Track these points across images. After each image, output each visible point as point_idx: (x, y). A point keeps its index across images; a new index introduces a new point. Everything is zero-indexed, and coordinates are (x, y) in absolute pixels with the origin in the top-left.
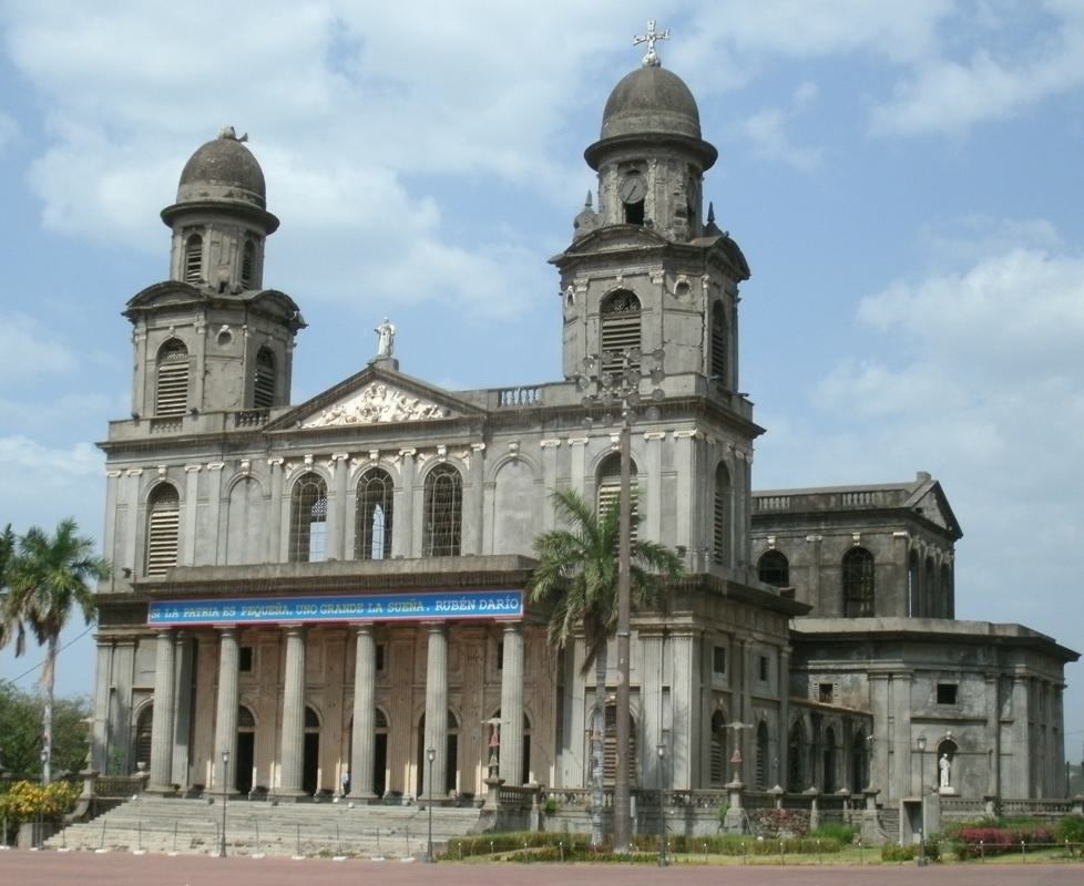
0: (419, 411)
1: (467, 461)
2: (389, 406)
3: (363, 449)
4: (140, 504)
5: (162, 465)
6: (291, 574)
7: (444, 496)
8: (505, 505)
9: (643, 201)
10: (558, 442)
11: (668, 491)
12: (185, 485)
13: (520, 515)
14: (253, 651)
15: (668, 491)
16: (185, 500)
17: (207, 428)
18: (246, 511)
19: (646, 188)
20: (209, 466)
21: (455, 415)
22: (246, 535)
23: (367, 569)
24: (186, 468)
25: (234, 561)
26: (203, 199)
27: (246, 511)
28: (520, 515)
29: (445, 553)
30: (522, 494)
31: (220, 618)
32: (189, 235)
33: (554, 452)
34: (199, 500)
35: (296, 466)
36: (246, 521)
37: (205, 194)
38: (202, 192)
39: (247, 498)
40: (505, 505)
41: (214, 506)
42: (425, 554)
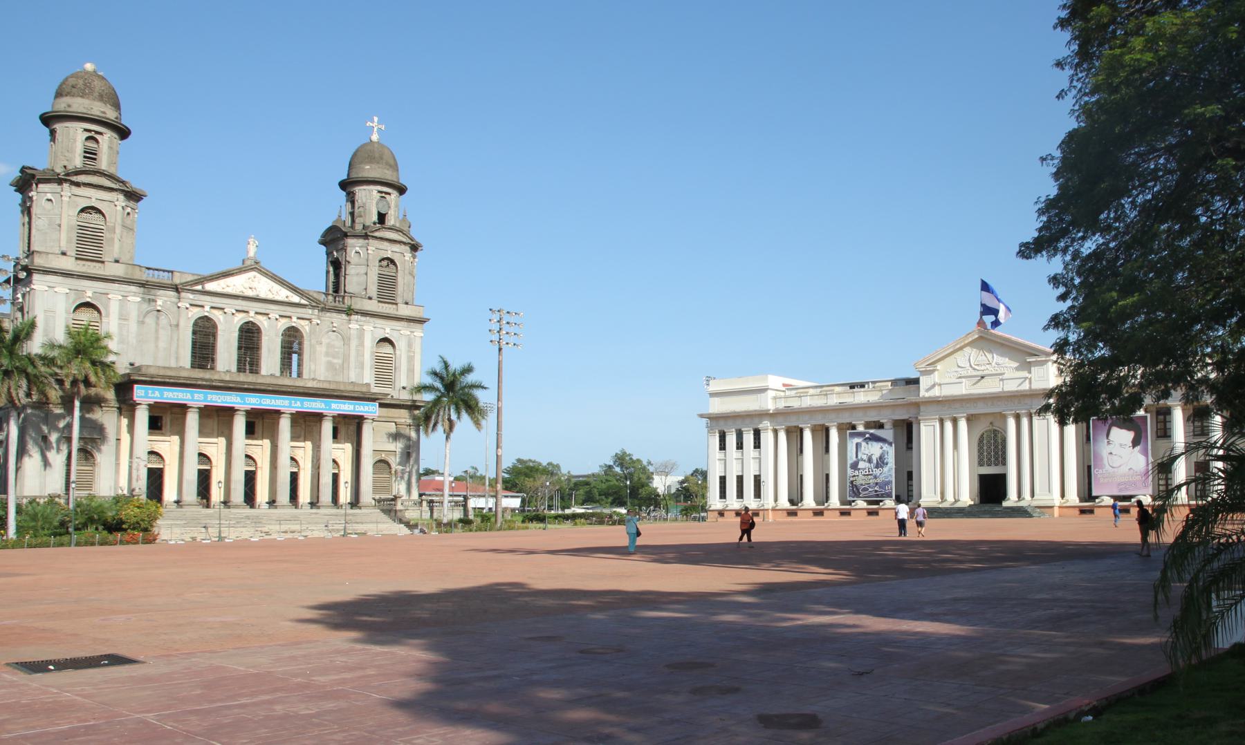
0: (283, 294)
1: (307, 328)
2: (265, 288)
3: (245, 309)
4: (67, 312)
5: (90, 291)
6: (237, 380)
7: (292, 343)
8: (327, 354)
9: (387, 213)
10: (358, 327)
11: (411, 359)
12: (107, 307)
13: (335, 361)
14: (164, 418)
15: (411, 359)
16: (108, 316)
17: (127, 274)
18: (157, 331)
19: (389, 207)
20: (129, 298)
21: (303, 302)
22: (157, 347)
23: (286, 381)
24: (109, 296)
25: (160, 364)
26: (104, 115)
27: (157, 331)
28: (335, 361)
29: (202, 367)
30: (337, 350)
31: (193, 400)
32: (88, 134)
33: (355, 332)
34: (120, 319)
35: (196, 310)
36: (157, 338)
37: (104, 113)
38: (102, 110)
39: (157, 324)
40: (327, 354)
41: (133, 326)
42: (193, 367)
